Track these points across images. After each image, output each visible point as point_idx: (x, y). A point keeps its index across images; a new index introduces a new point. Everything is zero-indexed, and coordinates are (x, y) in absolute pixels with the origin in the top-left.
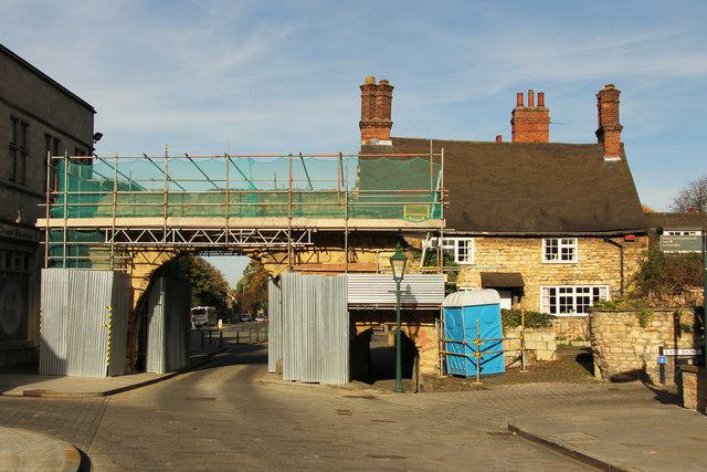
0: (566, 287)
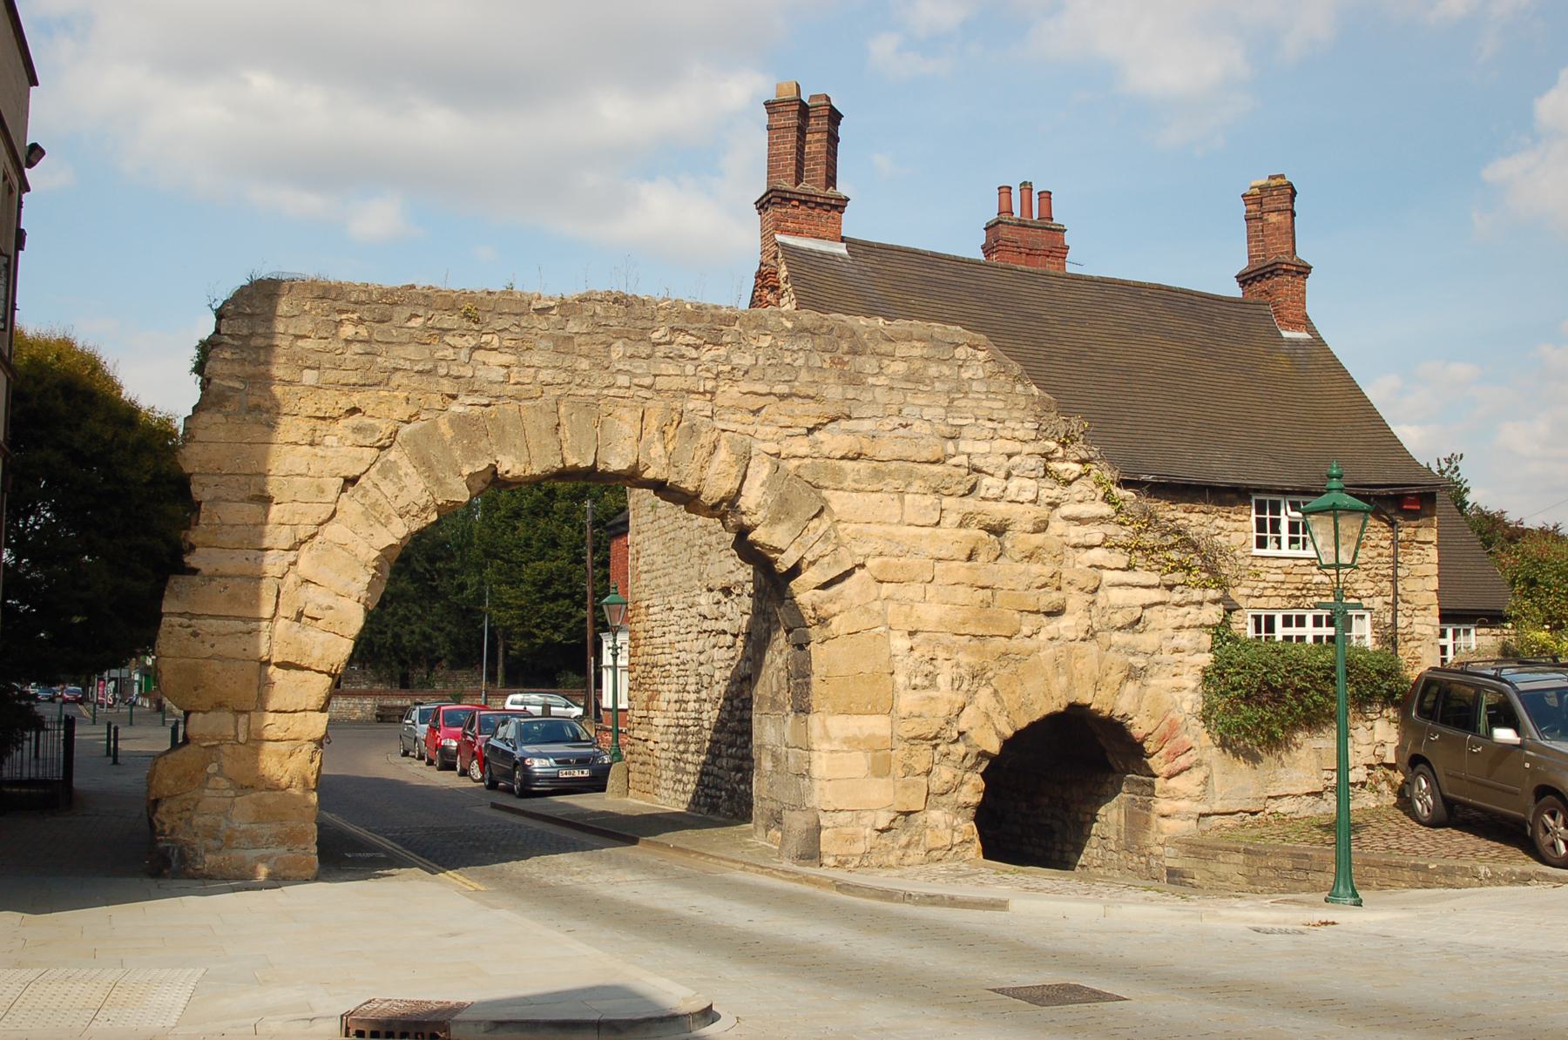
0: (1294, 613)
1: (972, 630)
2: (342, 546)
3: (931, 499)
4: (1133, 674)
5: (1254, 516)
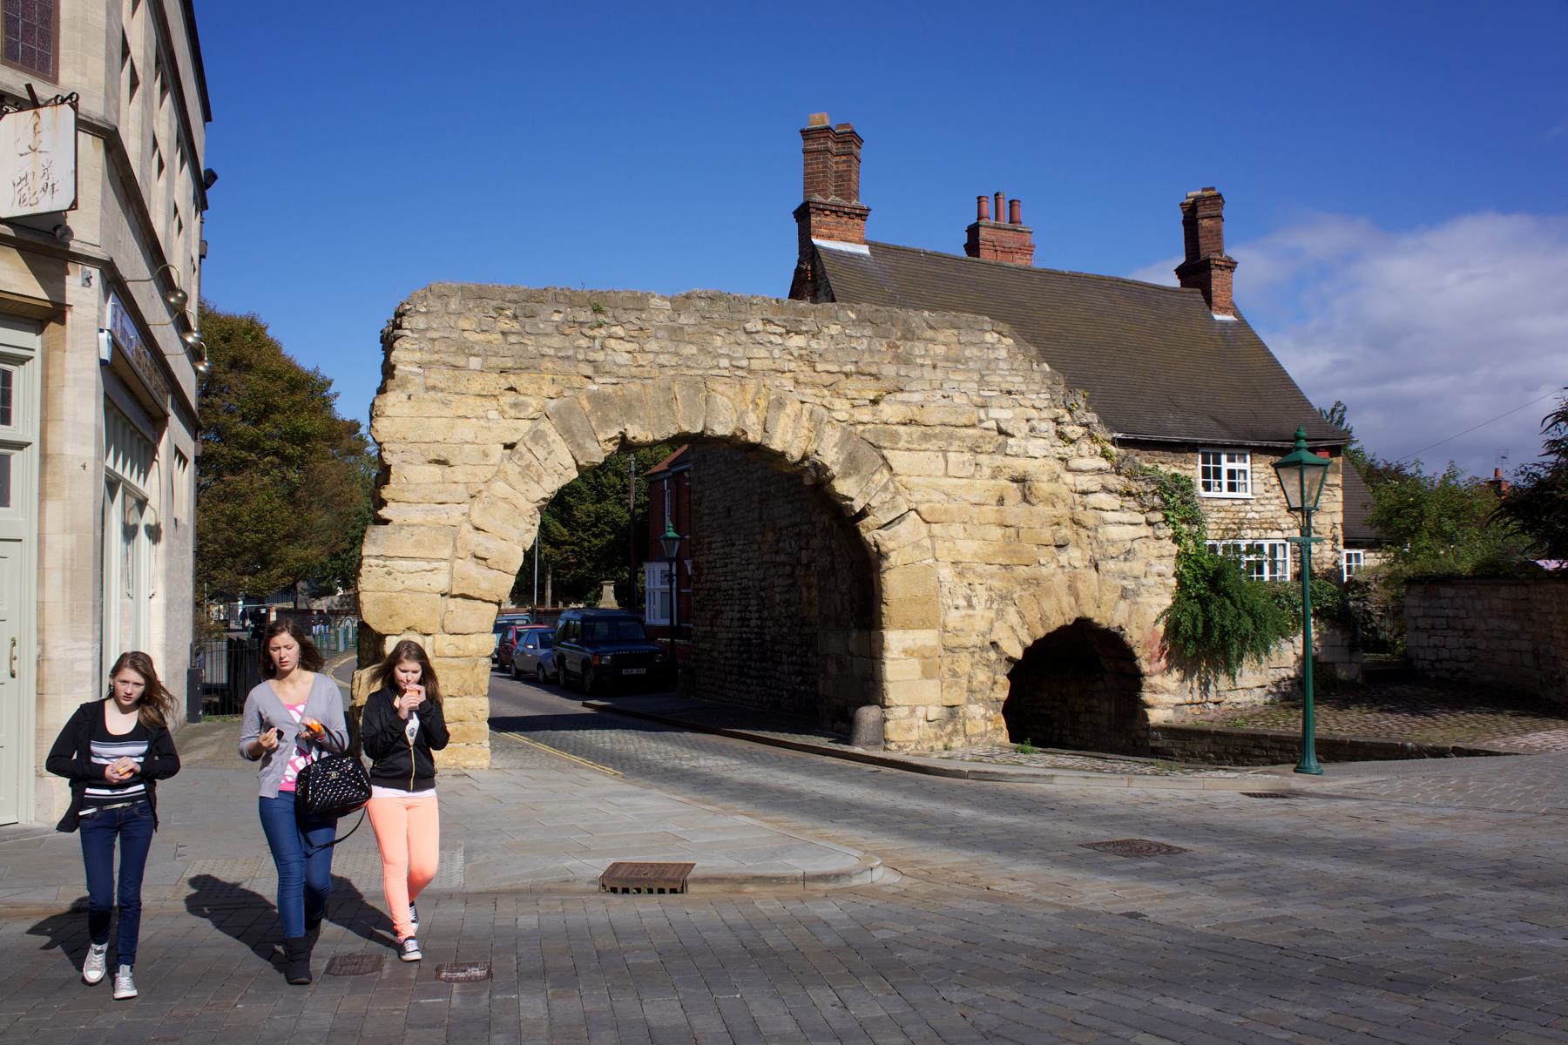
1: (1000, 560)
2: (504, 499)
3: (968, 456)
4: (1124, 594)
5: (1200, 465)
